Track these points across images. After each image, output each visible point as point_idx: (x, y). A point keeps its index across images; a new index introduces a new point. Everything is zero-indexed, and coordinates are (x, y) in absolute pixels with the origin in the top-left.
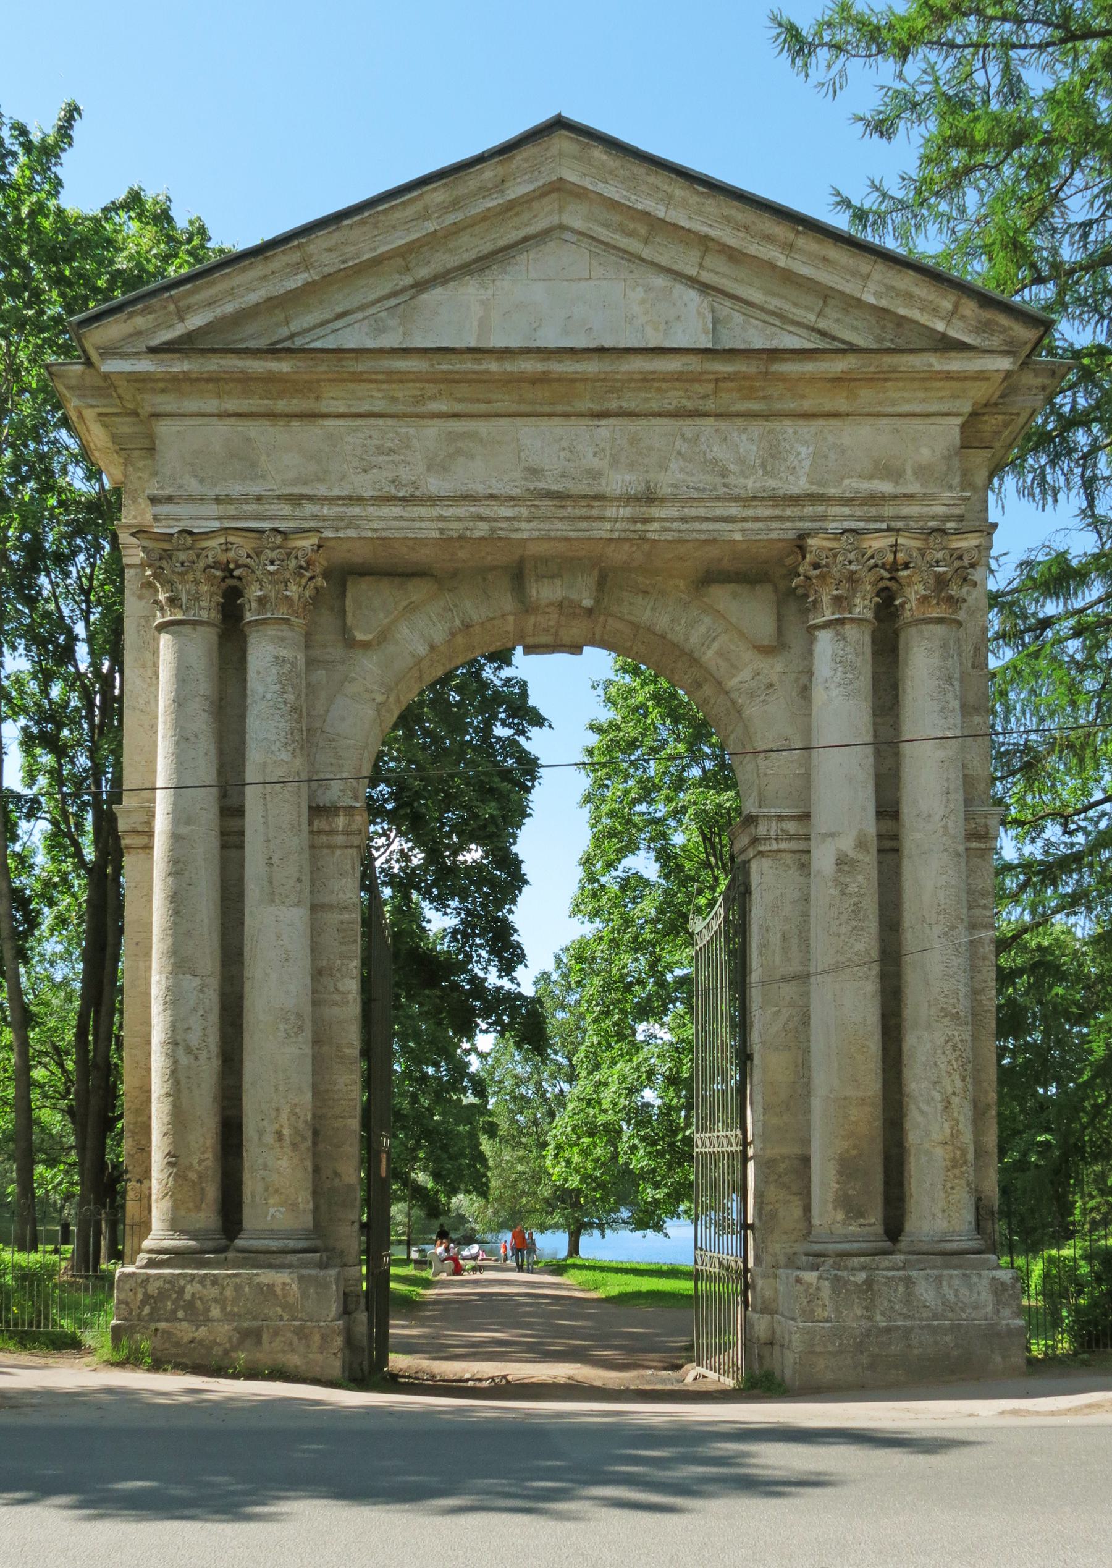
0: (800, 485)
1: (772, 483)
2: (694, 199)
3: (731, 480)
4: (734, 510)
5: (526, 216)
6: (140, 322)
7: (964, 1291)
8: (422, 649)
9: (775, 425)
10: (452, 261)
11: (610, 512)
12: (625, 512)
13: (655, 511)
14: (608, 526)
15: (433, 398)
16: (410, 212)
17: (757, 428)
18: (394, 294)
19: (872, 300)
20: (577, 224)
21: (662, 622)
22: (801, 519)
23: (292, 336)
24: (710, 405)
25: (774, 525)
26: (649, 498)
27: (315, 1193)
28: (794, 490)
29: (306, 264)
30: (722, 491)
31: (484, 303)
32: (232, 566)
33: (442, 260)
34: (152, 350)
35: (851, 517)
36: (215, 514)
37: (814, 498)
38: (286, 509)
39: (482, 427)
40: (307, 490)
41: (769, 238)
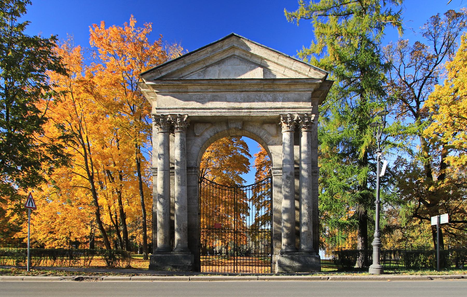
5: (227, 53)
6: (152, 74)
8: (209, 137)
9: (275, 93)
10: (213, 62)
11: (243, 111)
12: (246, 111)
15: (209, 89)
16: (204, 52)
18: (202, 68)
21: (255, 131)
22: (280, 112)
23: (183, 77)
24: (263, 89)
27: (189, 240)
29: (184, 63)
31: (219, 70)
33: (211, 62)
34: (155, 80)
35: (290, 111)
38: (182, 111)
39: (219, 94)
40: (186, 107)
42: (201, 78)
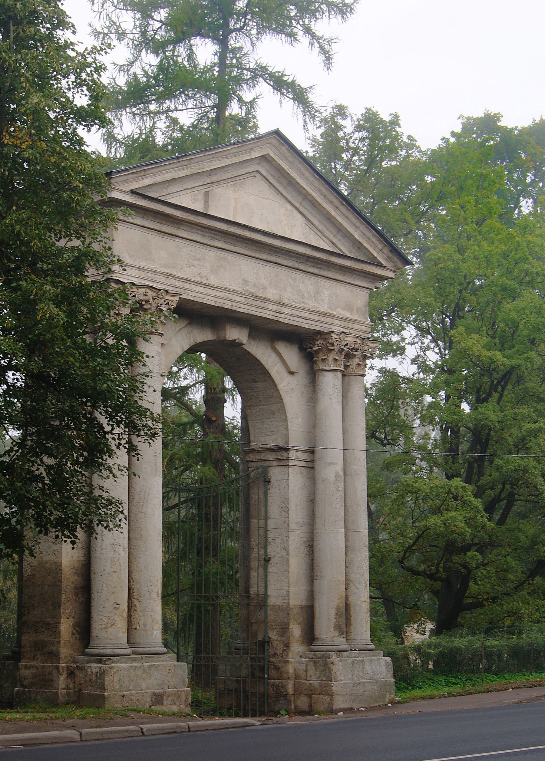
0: (324, 309)
1: (317, 305)
2: (311, 179)
3: (306, 301)
4: (306, 315)
7: (378, 666)
11: (270, 307)
12: (275, 308)
13: (285, 310)
14: (268, 312)
17: (314, 279)
19: (357, 237)
20: (264, 172)
22: (326, 323)
25: (318, 324)
26: (283, 305)
28: (323, 310)
30: (302, 305)
32: (144, 303)
36: (137, 275)
37: (325, 315)
38: (163, 279)
41: (331, 202)
42: (198, 207)
